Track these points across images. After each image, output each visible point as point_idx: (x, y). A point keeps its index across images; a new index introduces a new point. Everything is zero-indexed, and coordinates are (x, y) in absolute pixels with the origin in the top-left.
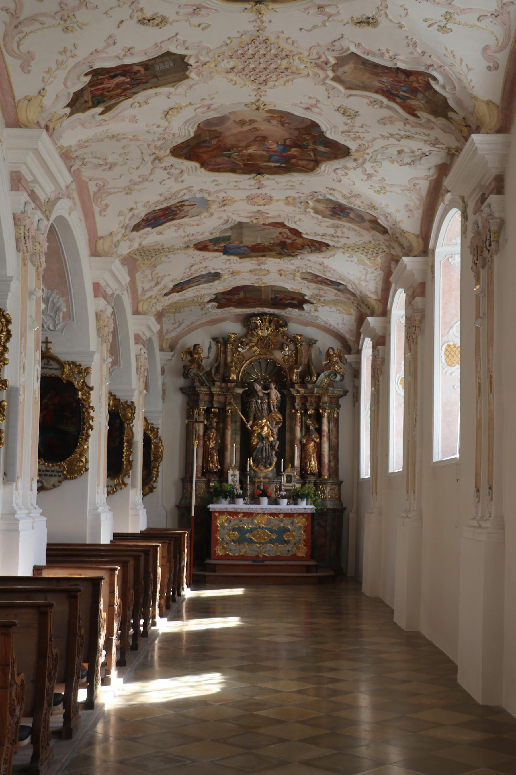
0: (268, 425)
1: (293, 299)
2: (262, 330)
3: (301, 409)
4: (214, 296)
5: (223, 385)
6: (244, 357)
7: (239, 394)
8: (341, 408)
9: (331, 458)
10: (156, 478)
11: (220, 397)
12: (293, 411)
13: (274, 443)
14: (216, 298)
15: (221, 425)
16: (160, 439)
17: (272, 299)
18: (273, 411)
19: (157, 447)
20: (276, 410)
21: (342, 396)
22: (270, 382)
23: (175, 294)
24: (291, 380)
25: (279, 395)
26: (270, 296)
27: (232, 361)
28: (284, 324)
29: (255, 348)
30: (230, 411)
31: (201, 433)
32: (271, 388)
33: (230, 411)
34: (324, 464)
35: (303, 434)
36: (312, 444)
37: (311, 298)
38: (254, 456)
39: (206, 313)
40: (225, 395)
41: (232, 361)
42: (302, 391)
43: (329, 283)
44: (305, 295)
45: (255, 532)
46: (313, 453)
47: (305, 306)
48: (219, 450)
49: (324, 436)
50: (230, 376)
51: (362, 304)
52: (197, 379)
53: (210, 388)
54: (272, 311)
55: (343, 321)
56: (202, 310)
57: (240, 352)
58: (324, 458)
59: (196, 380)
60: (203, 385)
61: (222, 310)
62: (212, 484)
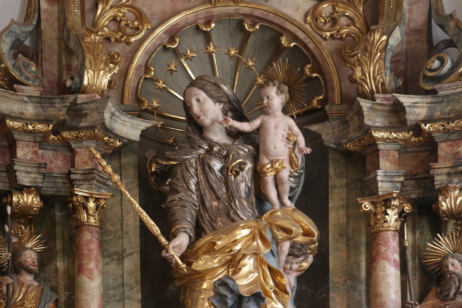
12: (367, 206)
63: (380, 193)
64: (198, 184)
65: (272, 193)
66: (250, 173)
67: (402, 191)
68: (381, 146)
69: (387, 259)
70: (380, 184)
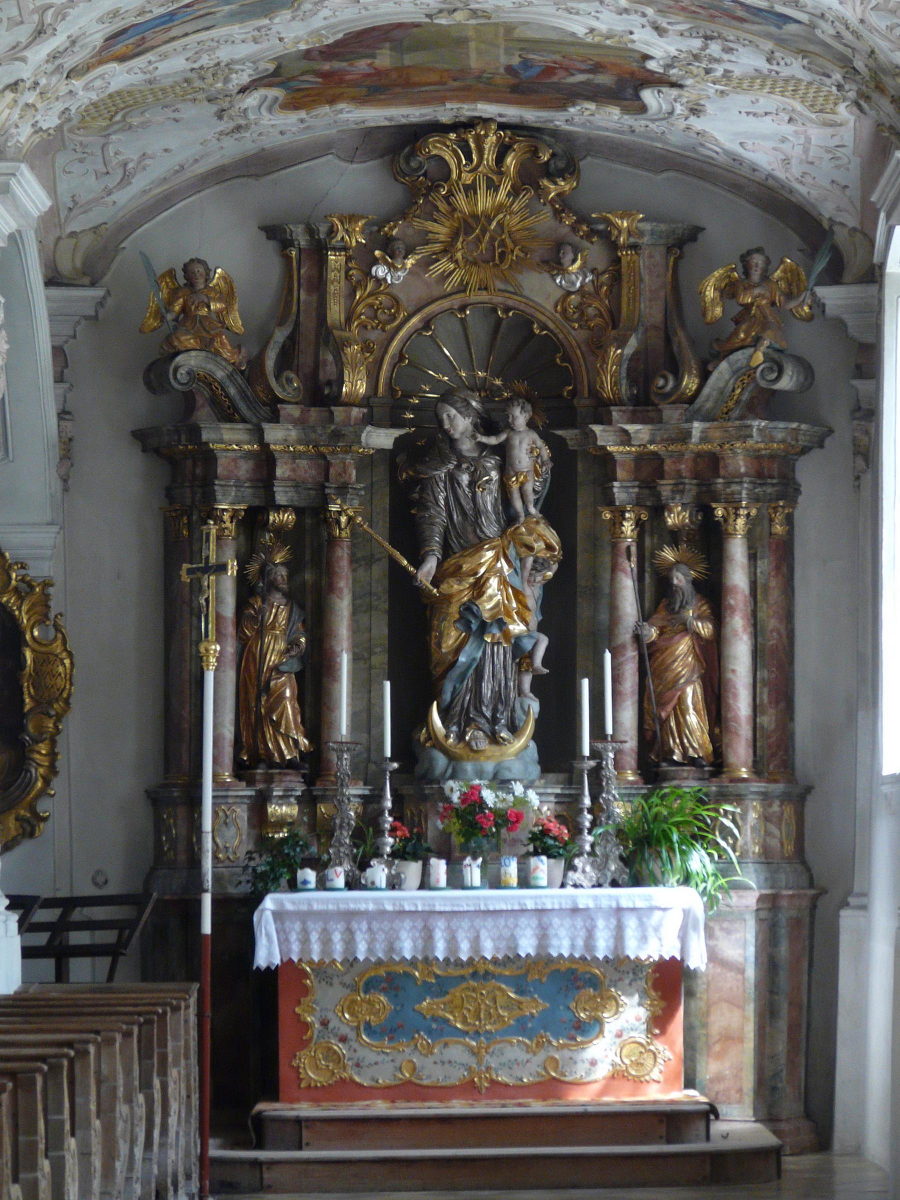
0: (500, 573)
1: (597, 68)
2: (471, 189)
3: (638, 503)
4: (271, 67)
5: (314, 413)
6: (396, 301)
7: (380, 451)
8: (800, 499)
9: (765, 696)
10: (47, 782)
11: (303, 463)
13: (528, 644)
14: (276, 73)
15: (308, 576)
16: (57, 628)
17: (509, 69)
18: (522, 519)
19: (45, 659)
20: (533, 510)
21: (805, 451)
22: (509, 401)
23: (113, 66)
24: (594, 394)
25: (546, 453)
26: (504, 60)
27: (349, 320)
28: (561, 164)
29: (444, 265)
30: (343, 519)
31: (229, 610)
32: (510, 427)
33: (343, 519)
34: (736, 719)
35: (647, 605)
36: (684, 646)
37: (669, 66)
38: (447, 697)
39: (238, 128)
40: (323, 456)
41: (349, 320)
42: (639, 431)
43: (740, 13)
44: (647, 57)
45: (457, 992)
46: (688, 682)
47: (648, 96)
48: (300, 677)
49: (733, 609)
50: (341, 382)
51: (875, 96)
52: (207, 393)
53: (258, 434)
54: (512, 113)
55: (806, 151)
56: (220, 117)
57: (379, 281)
58: (735, 696)
59: (200, 401)
60: (230, 420)
61: (303, 114)
62: (276, 810)
63: (617, 504)
64: (446, 499)
65: (518, 504)
66: (497, 485)
67: (637, 499)
68: (618, 457)
69: (624, 571)
70: (616, 495)
